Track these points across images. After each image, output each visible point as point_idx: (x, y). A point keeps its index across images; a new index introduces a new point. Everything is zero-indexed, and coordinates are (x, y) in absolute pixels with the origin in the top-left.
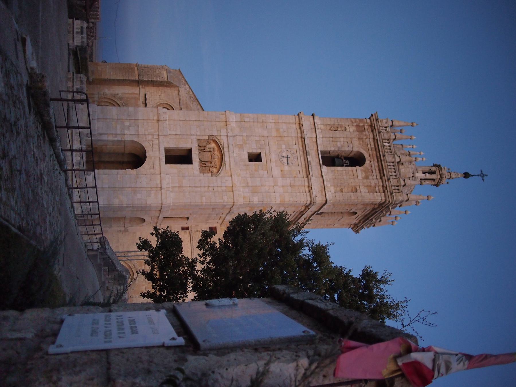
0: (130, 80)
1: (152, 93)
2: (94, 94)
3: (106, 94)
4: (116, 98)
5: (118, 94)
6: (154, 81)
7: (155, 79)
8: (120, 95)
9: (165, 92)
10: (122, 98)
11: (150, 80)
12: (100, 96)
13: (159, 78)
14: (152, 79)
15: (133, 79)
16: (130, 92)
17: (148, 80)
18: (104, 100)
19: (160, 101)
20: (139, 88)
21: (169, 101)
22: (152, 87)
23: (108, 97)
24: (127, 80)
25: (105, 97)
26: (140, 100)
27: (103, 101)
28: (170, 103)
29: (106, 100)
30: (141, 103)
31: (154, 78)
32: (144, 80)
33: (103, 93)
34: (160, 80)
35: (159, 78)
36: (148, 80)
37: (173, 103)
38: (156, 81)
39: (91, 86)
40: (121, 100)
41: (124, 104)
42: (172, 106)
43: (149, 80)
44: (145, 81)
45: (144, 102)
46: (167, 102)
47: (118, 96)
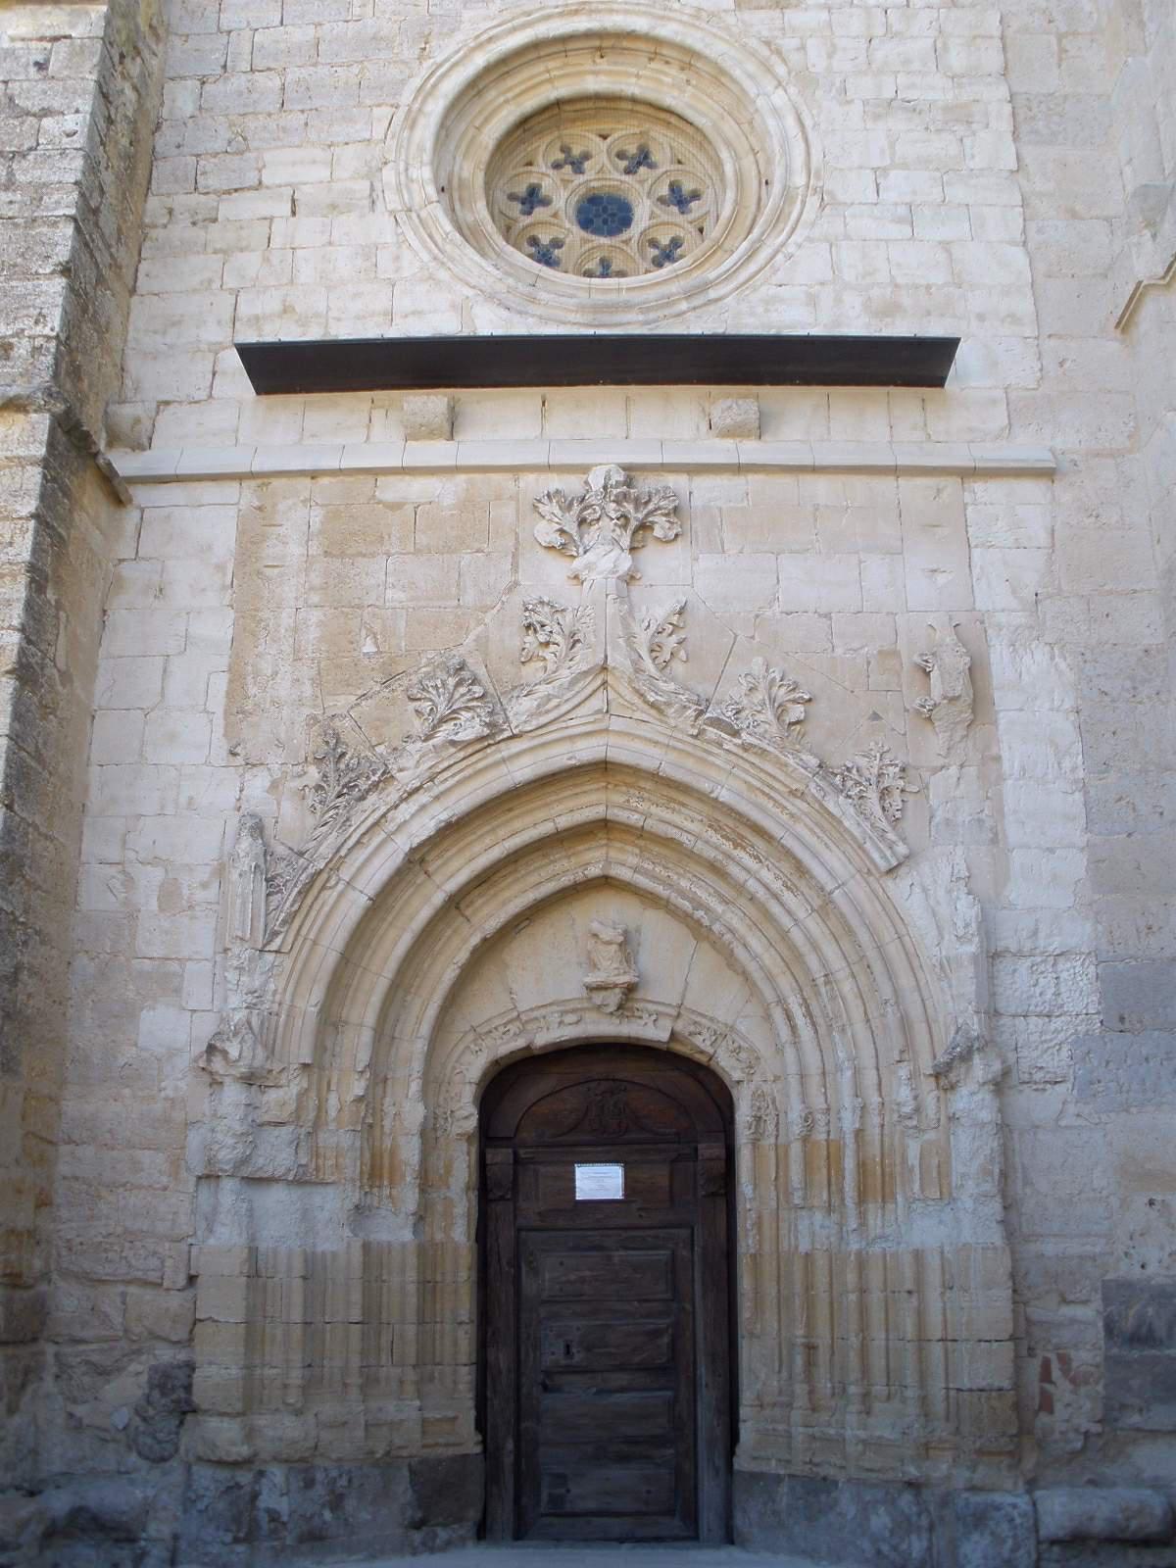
0: (37, 549)
1: (244, 310)
2: (255, 1270)
3: (268, 1038)
4: (336, 862)
5: (258, 829)
6: (87, 218)
7: (72, 169)
8: (274, 786)
9: (239, 146)
10: (332, 752)
11: (62, 241)
12: (278, 1153)
13: (46, 112)
14: (66, 204)
15: (30, 505)
16: (217, 627)
17: (66, 270)
18: (358, 1088)
19: (393, 201)
20: (141, 495)
21: (406, 97)
22: (142, 312)
23: (311, 1001)
24: (29, 606)
25: (302, 1050)
26: (375, 472)
27: (370, 1103)
28: (425, 93)
29: (358, 1044)
30: (438, 452)
31: (39, 191)
32: (54, 322)
33: (233, 1095)
34: (86, 104)
35: (47, 122)
36: (66, 270)
37: (444, 50)
38: (92, 167)
39: (68, 1301)
40: (388, 777)
41: (470, 727)
42: (480, 60)
43: (63, 253)
44: (71, 324)
45: (430, 403)
46: (411, 122)
47: (291, 818)
